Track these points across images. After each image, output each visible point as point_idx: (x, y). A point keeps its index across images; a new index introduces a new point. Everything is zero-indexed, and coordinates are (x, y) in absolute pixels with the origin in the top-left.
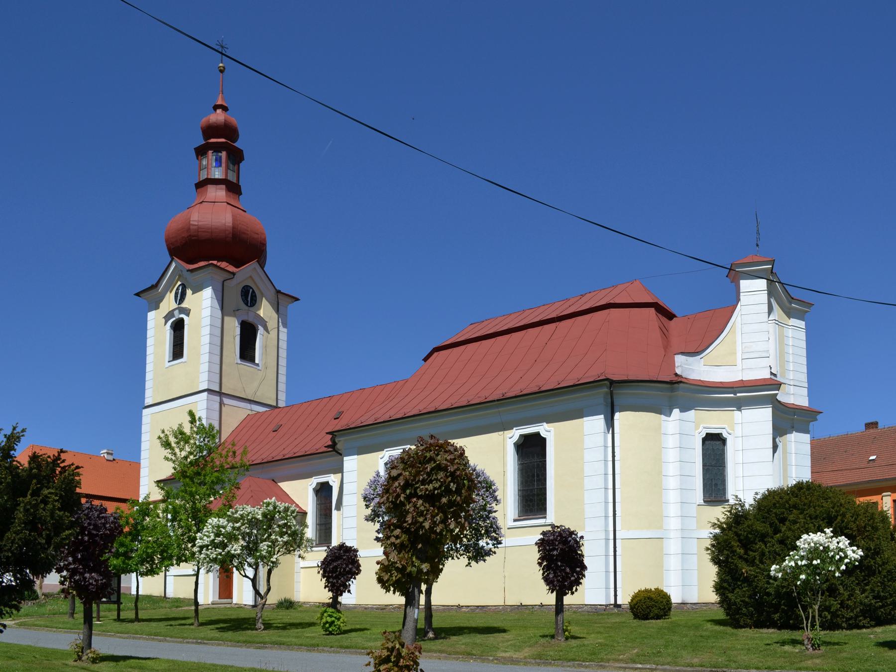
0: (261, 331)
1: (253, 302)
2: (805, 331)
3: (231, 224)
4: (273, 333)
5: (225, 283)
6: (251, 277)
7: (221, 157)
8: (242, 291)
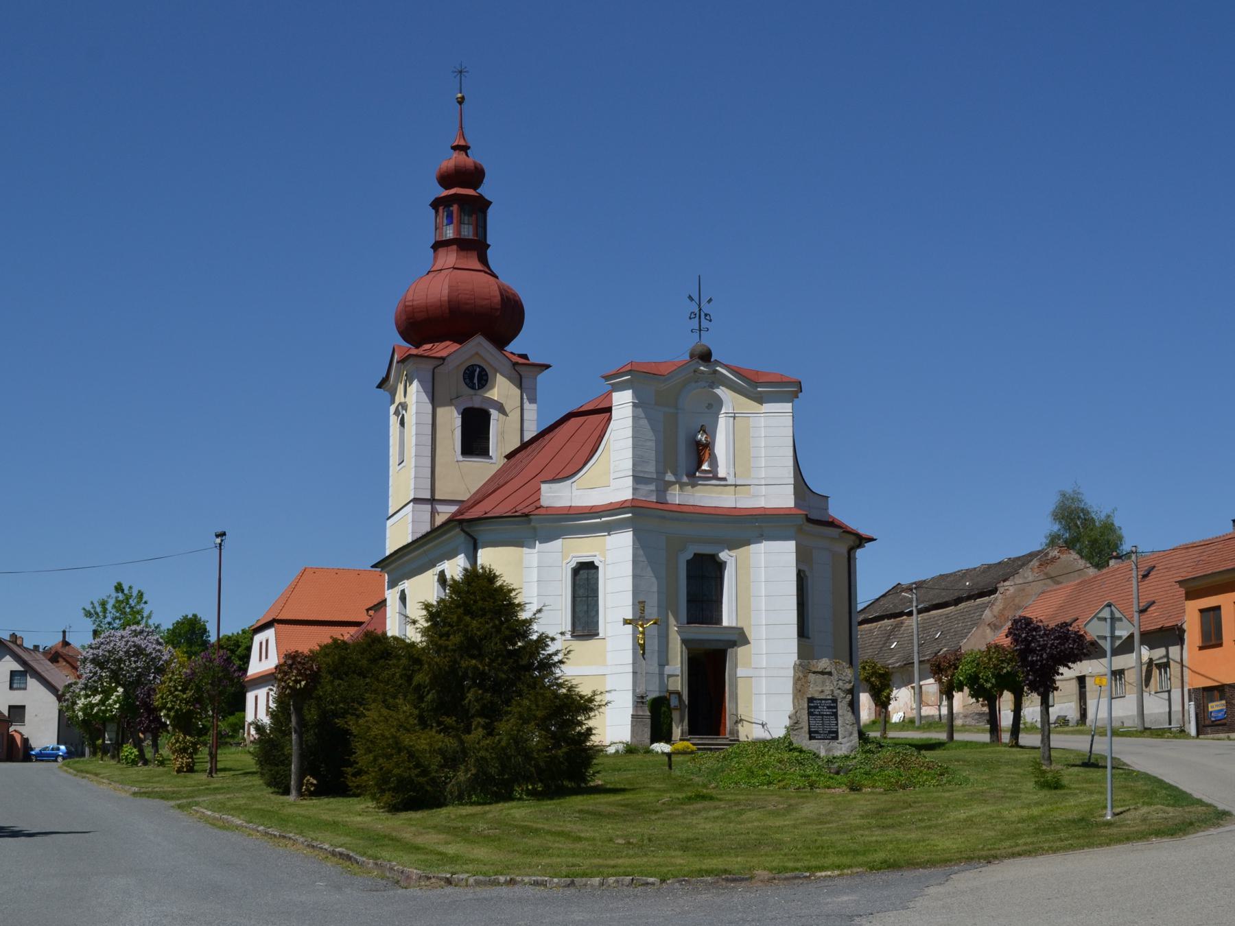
0: (494, 414)
1: (483, 382)
3: (446, 298)
4: (515, 416)
5: (435, 371)
6: (477, 353)
7: (452, 211)
8: (465, 373)
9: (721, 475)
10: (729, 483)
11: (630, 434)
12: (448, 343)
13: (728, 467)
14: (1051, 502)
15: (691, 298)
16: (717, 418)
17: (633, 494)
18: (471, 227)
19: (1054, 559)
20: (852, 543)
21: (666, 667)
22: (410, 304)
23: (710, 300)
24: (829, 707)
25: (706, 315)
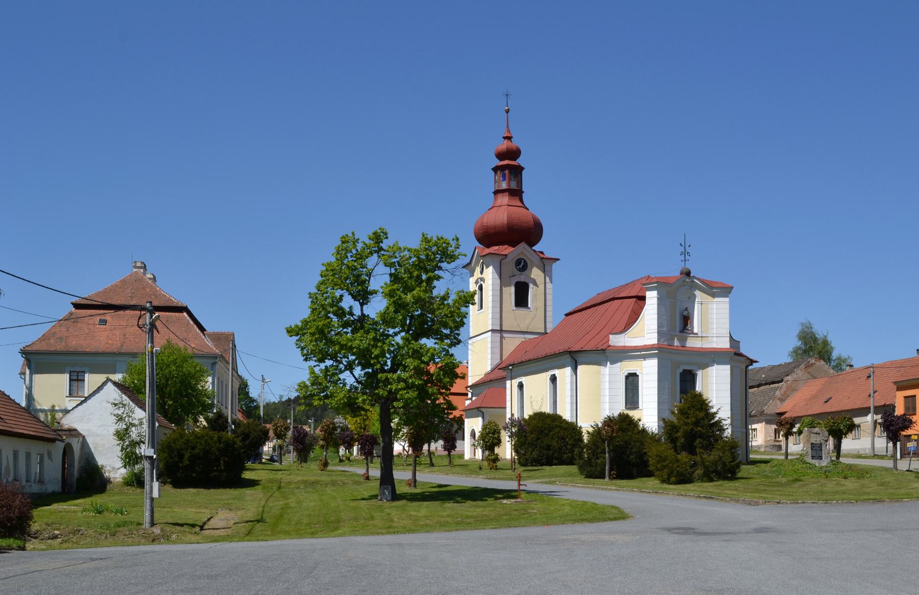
0: (531, 286)
3: (506, 222)
4: (542, 287)
6: (522, 252)
7: (505, 174)
8: (516, 263)
11: (656, 312)
12: (506, 246)
13: (698, 328)
14: (796, 330)
15: (681, 245)
16: (694, 304)
17: (658, 341)
18: (515, 182)
19: (812, 364)
20: (748, 364)
22: (486, 224)
23: (689, 246)
24: (819, 447)
25: (688, 253)
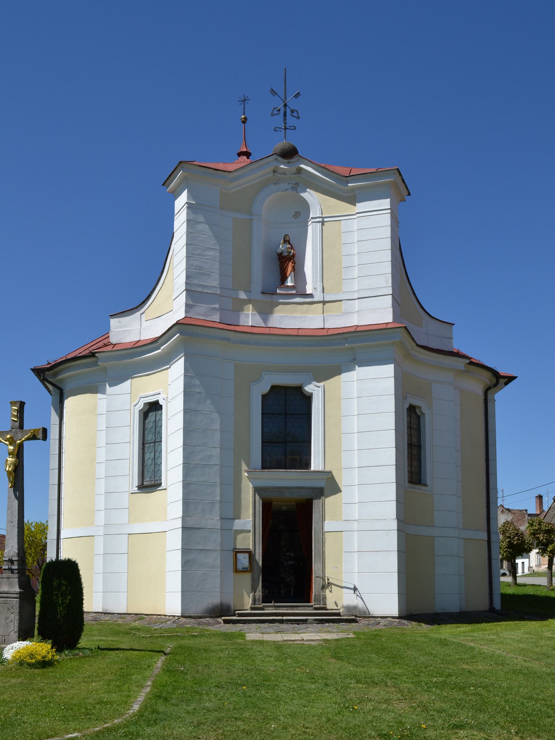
2: (389, 211)
9: (309, 291)
10: (316, 299)
13: (315, 282)
15: (273, 92)
16: (307, 226)
17: (186, 312)
21: (237, 521)
25: (292, 111)
